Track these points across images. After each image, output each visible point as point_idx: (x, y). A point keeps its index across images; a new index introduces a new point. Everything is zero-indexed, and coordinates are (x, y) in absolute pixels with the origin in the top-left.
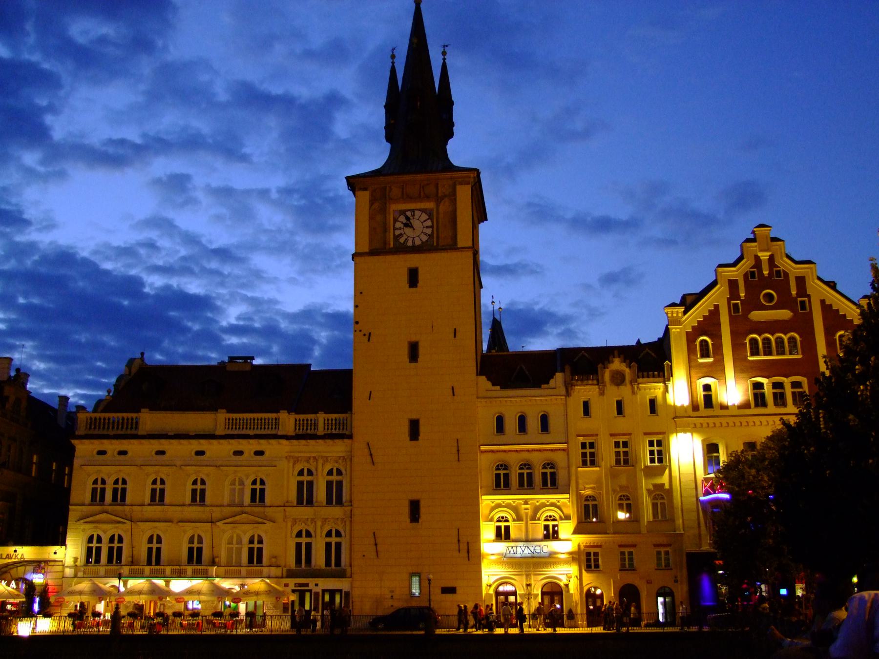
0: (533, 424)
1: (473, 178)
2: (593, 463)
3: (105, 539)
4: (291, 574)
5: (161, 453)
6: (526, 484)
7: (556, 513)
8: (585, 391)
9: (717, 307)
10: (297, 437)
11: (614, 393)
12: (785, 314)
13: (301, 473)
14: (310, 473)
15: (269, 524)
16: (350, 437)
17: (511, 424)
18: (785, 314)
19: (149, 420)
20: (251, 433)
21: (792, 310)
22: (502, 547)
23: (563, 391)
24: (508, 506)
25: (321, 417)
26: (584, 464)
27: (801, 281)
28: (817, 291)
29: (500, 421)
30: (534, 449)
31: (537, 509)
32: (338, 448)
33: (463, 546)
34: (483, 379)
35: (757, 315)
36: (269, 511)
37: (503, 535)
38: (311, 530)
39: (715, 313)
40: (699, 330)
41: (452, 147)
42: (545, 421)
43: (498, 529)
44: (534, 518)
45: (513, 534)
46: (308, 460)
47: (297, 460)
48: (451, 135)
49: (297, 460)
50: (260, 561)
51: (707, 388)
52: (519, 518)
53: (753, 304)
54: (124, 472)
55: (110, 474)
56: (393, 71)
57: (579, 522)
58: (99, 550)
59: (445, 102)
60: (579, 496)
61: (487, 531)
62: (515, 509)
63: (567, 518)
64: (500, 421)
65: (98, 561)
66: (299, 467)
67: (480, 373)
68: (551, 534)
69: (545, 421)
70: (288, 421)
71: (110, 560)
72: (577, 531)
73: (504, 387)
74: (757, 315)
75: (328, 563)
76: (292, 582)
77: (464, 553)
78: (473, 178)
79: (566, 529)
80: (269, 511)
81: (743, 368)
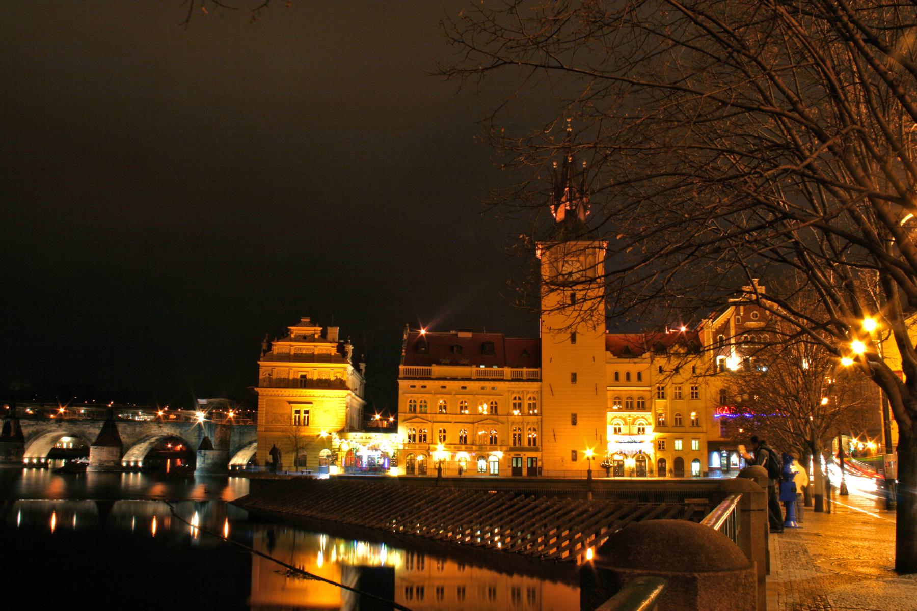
0: (634, 377)
2: (663, 397)
3: (418, 430)
4: (512, 449)
5: (464, 388)
6: (629, 407)
7: (644, 422)
8: (661, 361)
9: (729, 320)
10: (513, 380)
11: (675, 362)
13: (515, 398)
14: (519, 399)
15: (501, 425)
16: (541, 381)
17: (622, 377)
19: (436, 369)
20: (490, 378)
22: (618, 438)
23: (649, 360)
24: (621, 418)
25: (525, 369)
26: (659, 397)
29: (617, 374)
30: (636, 390)
31: (635, 420)
32: (536, 385)
33: (599, 437)
34: (609, 353)
36: (500, 418)
37: (617, 431)
38: (521, 427)
39: (728, 322)
40: (718, 331)
42: (639, 375)
43: (615, 429)
44: (633, 424)
45: (623, 431)
46: (518, 392)
47: (513, 392)
49: (513, 392)
50: (496, 443)
51: (722, 361)
52: (626, 424)
54: (426, 397)
55: (418, 398)
57: (656, 426)
60: (655, 413)
61: (610, 429)
62: (624, 419)
63: (650, 424)
64: (617, 374)
66: (514, 395)
67: (607, 349)
68: (641, 430)
69: (639, 375)
70: (507, 371)
71: (420, 441)
72: (656, 430)
73: (620, 357)
76: (512, 453)
77: (599, 441)
79: (650, 429)
80: (500, 418)
81: (739, 351)
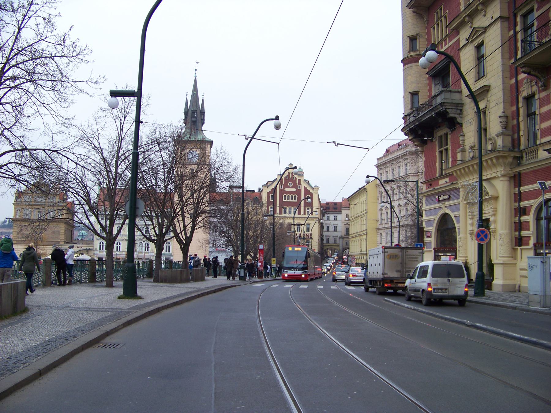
1: (211, 142)
12: (294, 190)
18: (294, 190)
21: (297, 188)
27: (299, 180)
28: (303, 184)
35: (287, 189)
41: (204, 127)
48: (203, 123)
53: (286, 186)
56: (187, 99)
58: (103, 246)
59: (203, 113)
65: (103, 249)
74: (287, 189)
75: (166, 251)
78: (211, 142)
